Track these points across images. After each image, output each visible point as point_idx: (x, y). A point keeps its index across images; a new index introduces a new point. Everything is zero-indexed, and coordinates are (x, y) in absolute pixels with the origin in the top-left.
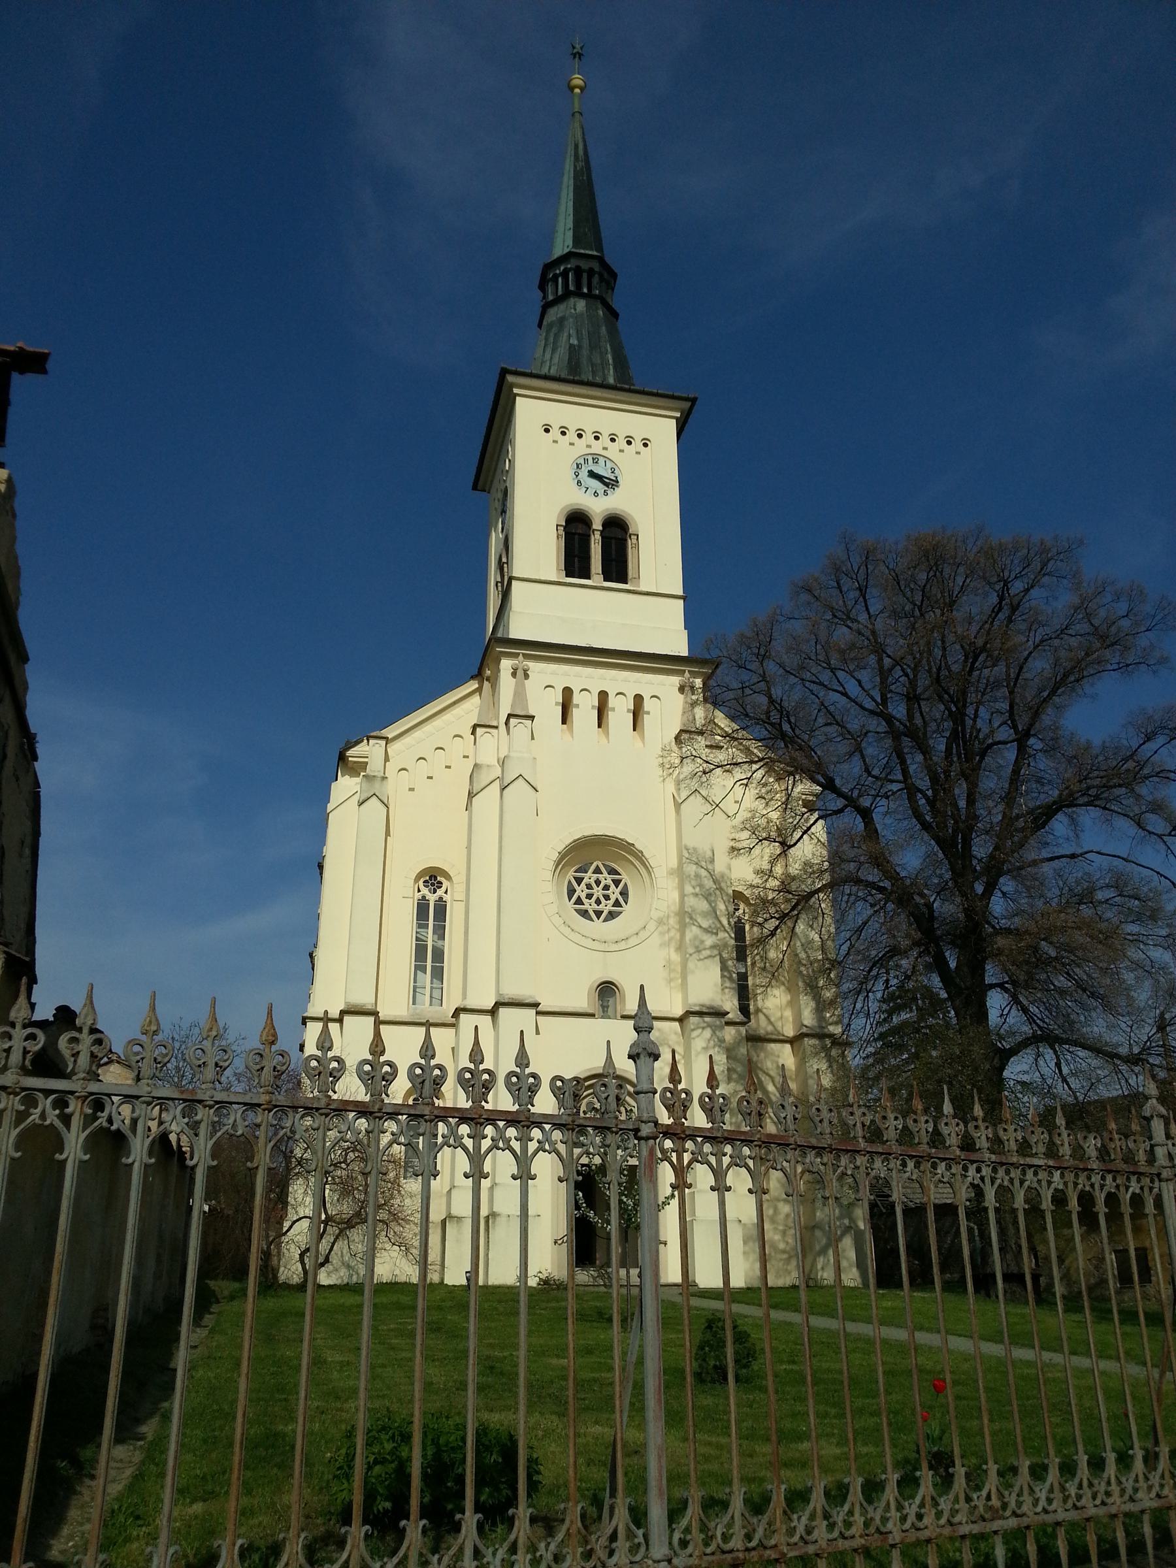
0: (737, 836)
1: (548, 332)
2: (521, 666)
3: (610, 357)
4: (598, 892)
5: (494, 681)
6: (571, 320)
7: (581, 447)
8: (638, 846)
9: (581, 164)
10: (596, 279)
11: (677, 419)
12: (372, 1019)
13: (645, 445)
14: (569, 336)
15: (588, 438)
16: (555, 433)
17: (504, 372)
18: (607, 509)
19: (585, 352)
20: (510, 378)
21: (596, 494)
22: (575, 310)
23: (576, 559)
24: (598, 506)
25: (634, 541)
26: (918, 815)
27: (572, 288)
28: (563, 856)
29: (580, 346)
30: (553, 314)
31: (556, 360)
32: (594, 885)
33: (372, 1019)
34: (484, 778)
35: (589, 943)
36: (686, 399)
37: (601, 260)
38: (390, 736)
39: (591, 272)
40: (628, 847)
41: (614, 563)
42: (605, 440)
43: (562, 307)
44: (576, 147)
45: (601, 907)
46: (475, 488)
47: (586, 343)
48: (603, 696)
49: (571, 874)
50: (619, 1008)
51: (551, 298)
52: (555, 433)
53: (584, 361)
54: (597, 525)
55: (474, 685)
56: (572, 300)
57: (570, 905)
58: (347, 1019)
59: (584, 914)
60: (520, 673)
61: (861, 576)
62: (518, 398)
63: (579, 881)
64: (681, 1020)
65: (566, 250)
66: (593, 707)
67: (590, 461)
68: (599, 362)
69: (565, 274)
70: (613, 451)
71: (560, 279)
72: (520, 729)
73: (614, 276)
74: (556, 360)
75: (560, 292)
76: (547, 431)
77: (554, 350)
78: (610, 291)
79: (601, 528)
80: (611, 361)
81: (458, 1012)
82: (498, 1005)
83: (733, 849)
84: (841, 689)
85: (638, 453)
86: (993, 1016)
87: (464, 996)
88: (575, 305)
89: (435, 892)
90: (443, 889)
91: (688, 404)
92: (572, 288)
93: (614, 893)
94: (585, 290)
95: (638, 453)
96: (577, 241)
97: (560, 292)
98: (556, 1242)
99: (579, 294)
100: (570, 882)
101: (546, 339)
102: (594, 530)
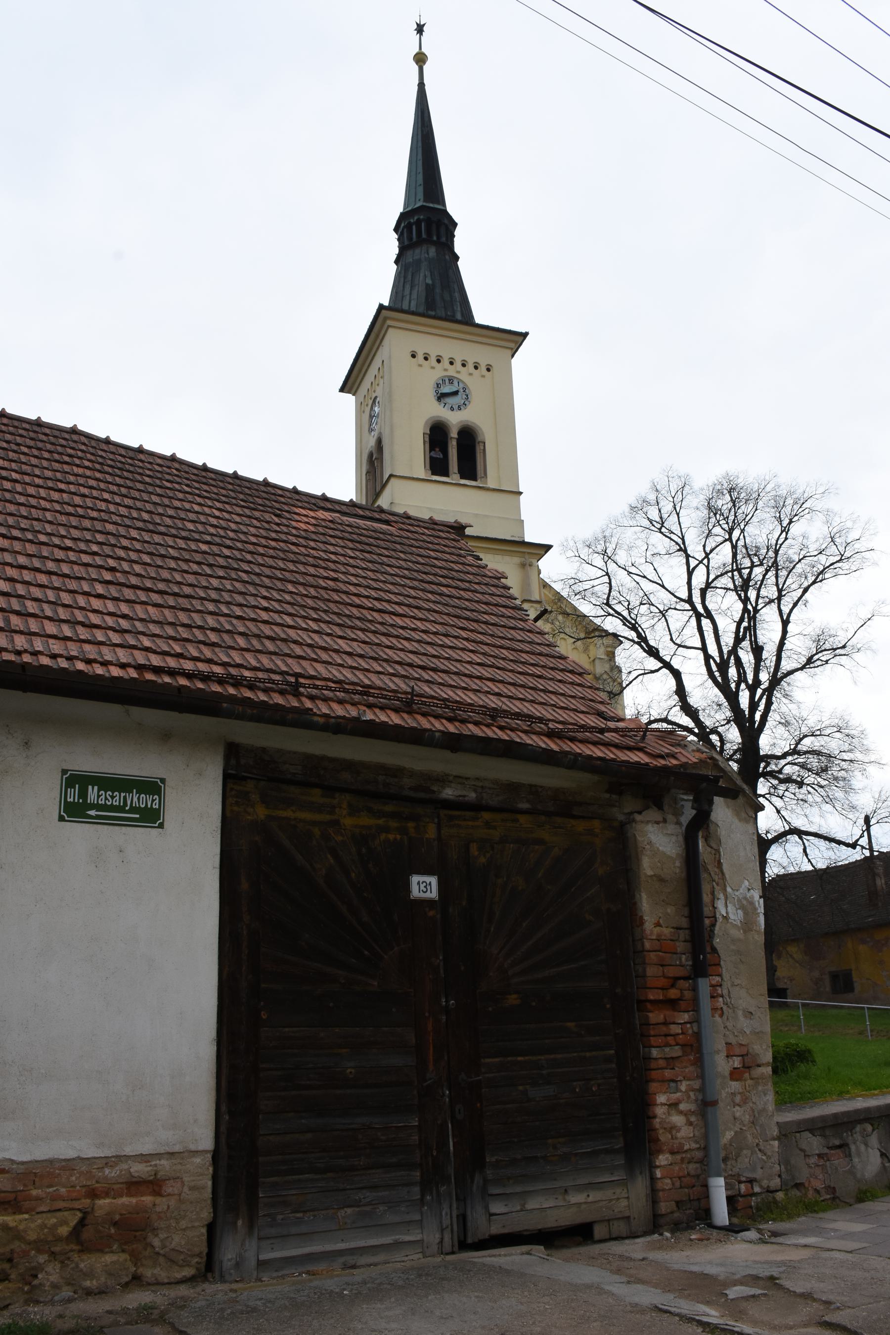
13: (488, 370)
14: (425, 276)
15: (445, 362)
18: (461, 422)
19: (438, 290)
22: (428, 254)
24: (455, 419)
27: (424, 236)
31: (414, 296)
42: (458, 364)
43: (417, 251)
54: (454, 434)
56: (424, 247)
69: (418, 223)
71: (414, 227)
74: (414, 296)
76: (413, 356)
77: (412, 287)
79: (456, 436)
88: (427, 251)
92: (424, 236)
94: (435, 238)
99: (429, 241)
102: (451, 438)
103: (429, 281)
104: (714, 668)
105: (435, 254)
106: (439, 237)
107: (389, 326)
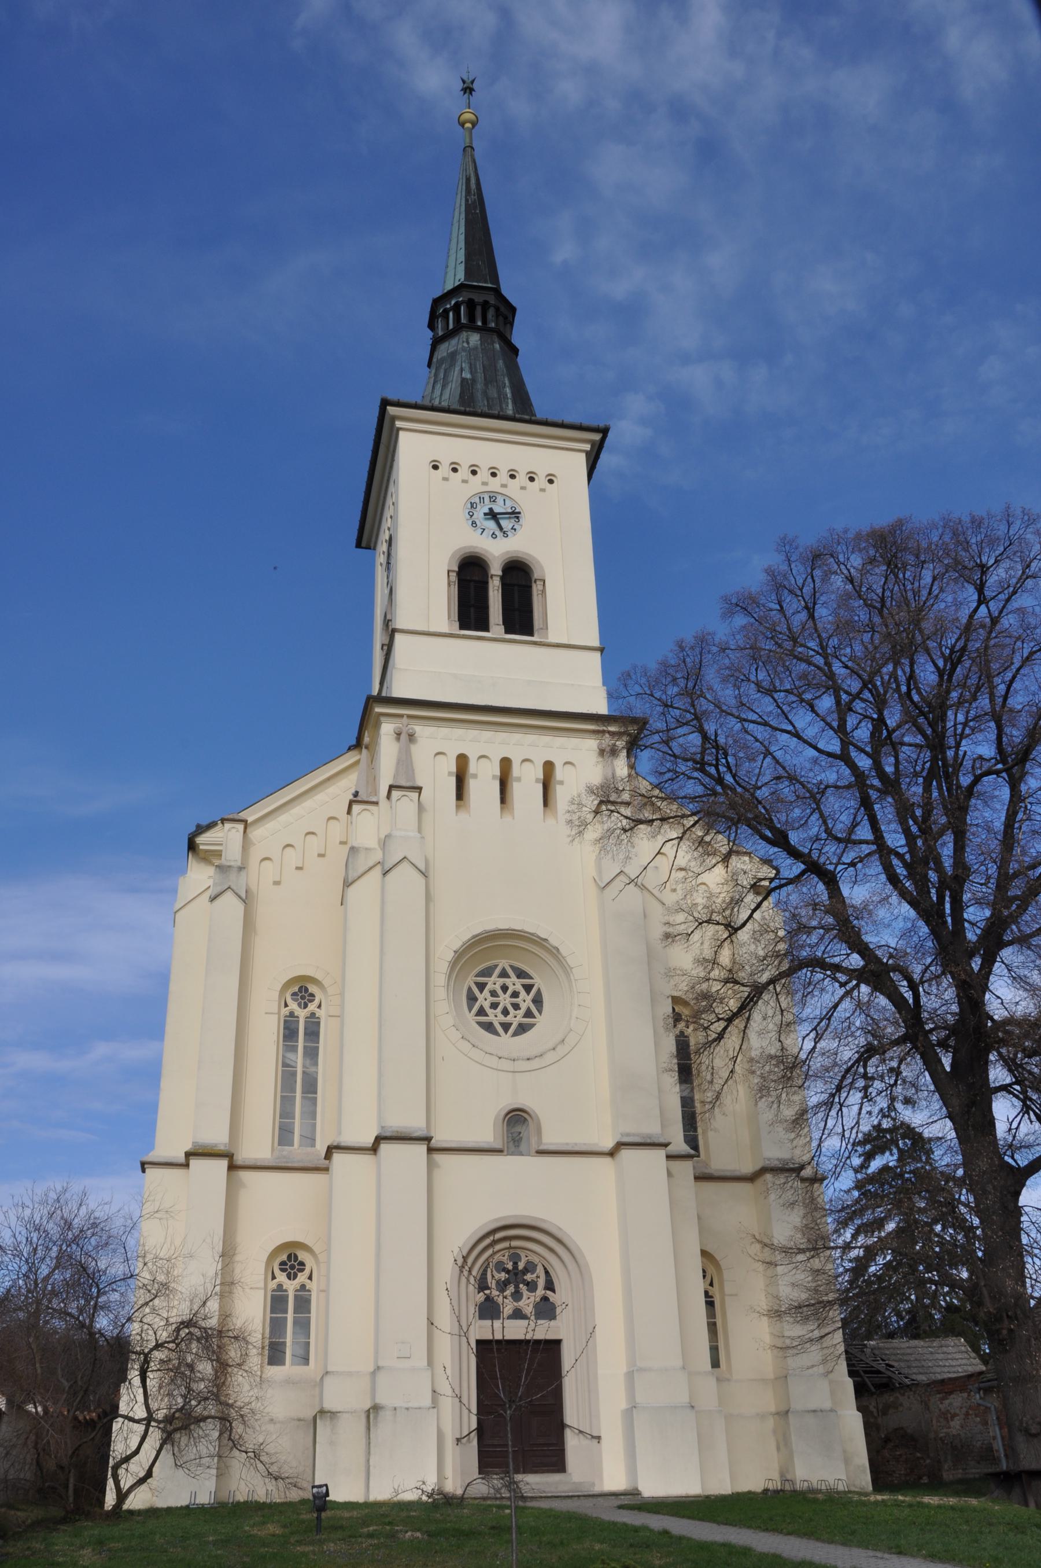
0: (671, 919)
1: (437, 369)
2: (405, 730)
3: (508, 390)
4: (505, 1000)
5: (372, 749)
6: (464, 354)
7: (476, 485)
8: (554, 941)
9: (473, 198)
10: (491, 313)
11: (588, 454)
12: (224, 1163)
14: (462, 370)
15: (484, 474)
16: (445, 469)
17: (385, 403)
18: (508, 552)
19: (480, 386)
20: (391, 410)
21: (494, 536)
22: (468, 343)
23: (472, 610)
25: (540, 588)
26: (893, 879)
27: (463, 320)
28: (459, 955)
30: (443, 350)
32: (500, 992)
33: (224, 1163)
34: (362, 863)
35: (493, 1061)
37: (497, 292)
38: (250, 820)
39: (485, 305)
40: (541, 942)
42: (503, 476)
43: (454, 342)
45: (509, 1019)
46: (359, 545)
47: (480, 377)
48: (506, 764)
49: (470, 981)
50: (534, 1141)
51: (440, 333)
52: (445, 469)
53: (479, 395)
54: (496, 569)
55: (351, 757)
56: (464, 335)
57: (471, 1017)
58: (194, 1162)
59: (489, 1027)
60: (404, 737)
61: (807, 590)
62: (401, 433)
63: (481, 987)
64: (612, 1153)
65: (457, 283)
66: (494, 777)
67: (487, 499)
68: (496, 395)
69: (456, 308)
70: (513, 488)
71: (451, 314)
72: (406, 803)
73: (513, 310)
75: (451, 326)
76: (436, 467)
77: (444, 387)
78: (508, 325)
79: (500, 573)
80: (509, 395)
81: (330, 1151)
82: (379, 1139)
83: (667, 936)
84: (790, 728)
85: (543, 490)
86: (1001, 1128)
87: (340, 1133)
89: (306, 1006)
90: (316, 1002)
91: (597, 437)
93: (526, 1001)
94: (479, 323)
95: (543, 490)
97: (451, 326)
98: (458, 1440)
99: (472, 327)
100: (470, 989)
101: (436, 375)
102: (492, 576)
103: (467, 375)
104: (901, 871)
105: (479, 343)
106: (485, 321)
107: (399, 429)
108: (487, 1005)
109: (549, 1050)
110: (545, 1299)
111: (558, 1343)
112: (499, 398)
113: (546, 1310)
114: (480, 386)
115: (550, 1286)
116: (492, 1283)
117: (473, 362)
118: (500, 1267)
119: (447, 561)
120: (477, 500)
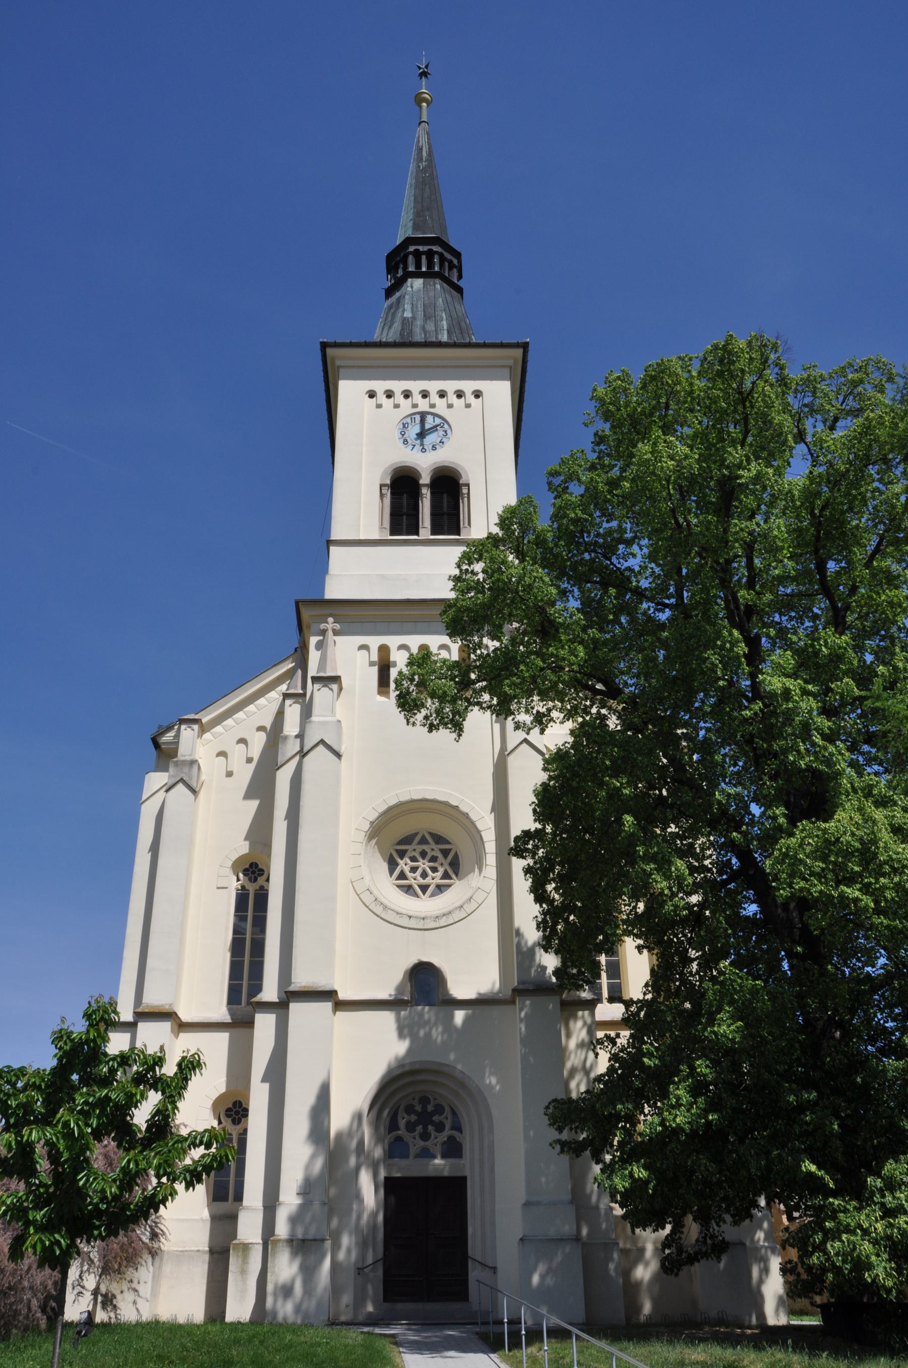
3: (445, 323)
17: (324, 346)
18: (435, 463)
19: (419, 322)
20: (330, 351)
22: (412, 287)
29: (414, 318)
36: (517, 345)
41: (446, 517)
44: (420, 150)
45: (428, 880)
47: (420, 314)
54: (425, 479)
59: (408, 889)
68: (433, 329)
70: (441, 406)
80: (445, 327)
89: (255, 880)
90: (264, 877)
94: (424, 269)
96: (416, 227)
108: (407, 869)
109: (456, 909)
110: (451, 1139)
111: (464, 1179)
112: (436, 330)
113: (453, 1150)
114: (419, 322)
115: (458, 1128)
116: (402, 1123)
117: (415, 303)
118: (409, 1110)
119: (379, 477)
120: (409, 420)
